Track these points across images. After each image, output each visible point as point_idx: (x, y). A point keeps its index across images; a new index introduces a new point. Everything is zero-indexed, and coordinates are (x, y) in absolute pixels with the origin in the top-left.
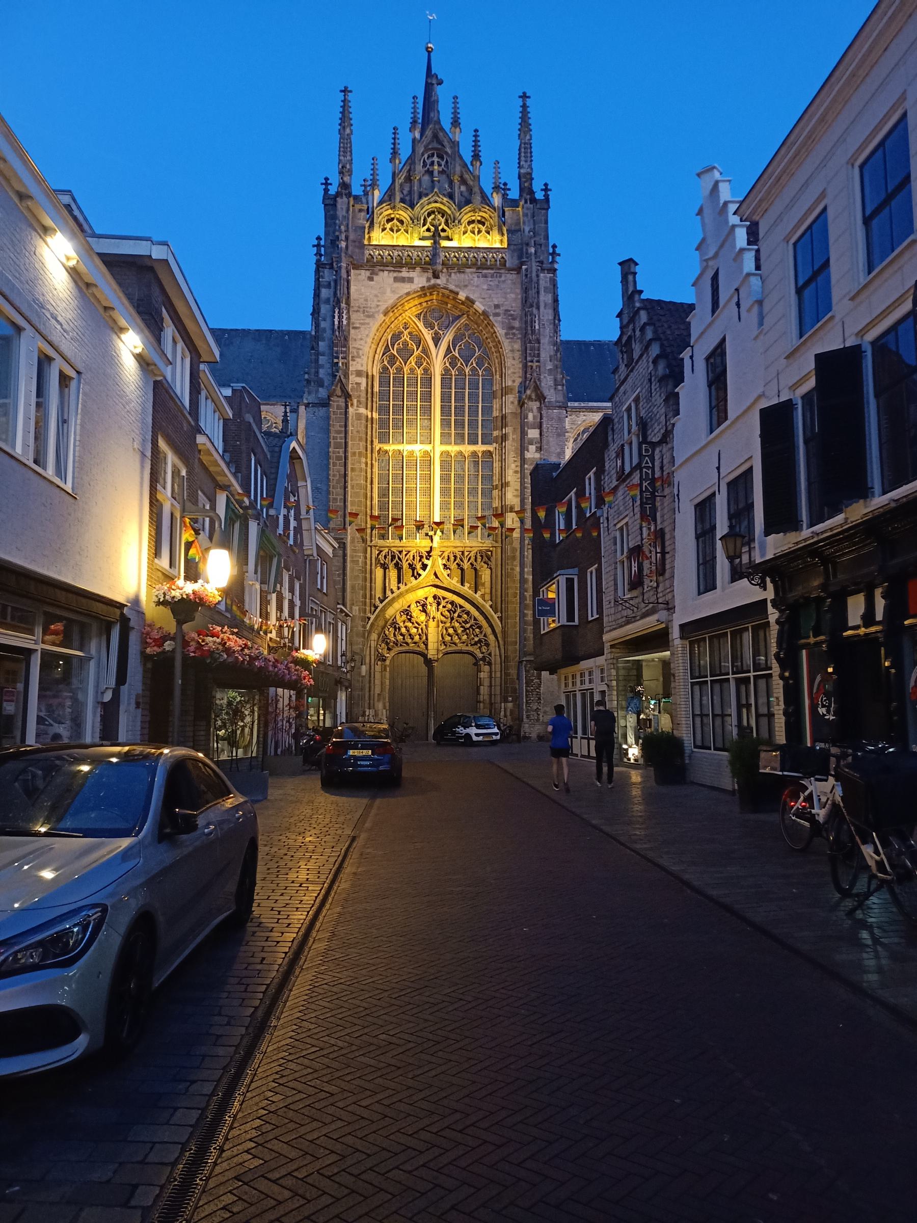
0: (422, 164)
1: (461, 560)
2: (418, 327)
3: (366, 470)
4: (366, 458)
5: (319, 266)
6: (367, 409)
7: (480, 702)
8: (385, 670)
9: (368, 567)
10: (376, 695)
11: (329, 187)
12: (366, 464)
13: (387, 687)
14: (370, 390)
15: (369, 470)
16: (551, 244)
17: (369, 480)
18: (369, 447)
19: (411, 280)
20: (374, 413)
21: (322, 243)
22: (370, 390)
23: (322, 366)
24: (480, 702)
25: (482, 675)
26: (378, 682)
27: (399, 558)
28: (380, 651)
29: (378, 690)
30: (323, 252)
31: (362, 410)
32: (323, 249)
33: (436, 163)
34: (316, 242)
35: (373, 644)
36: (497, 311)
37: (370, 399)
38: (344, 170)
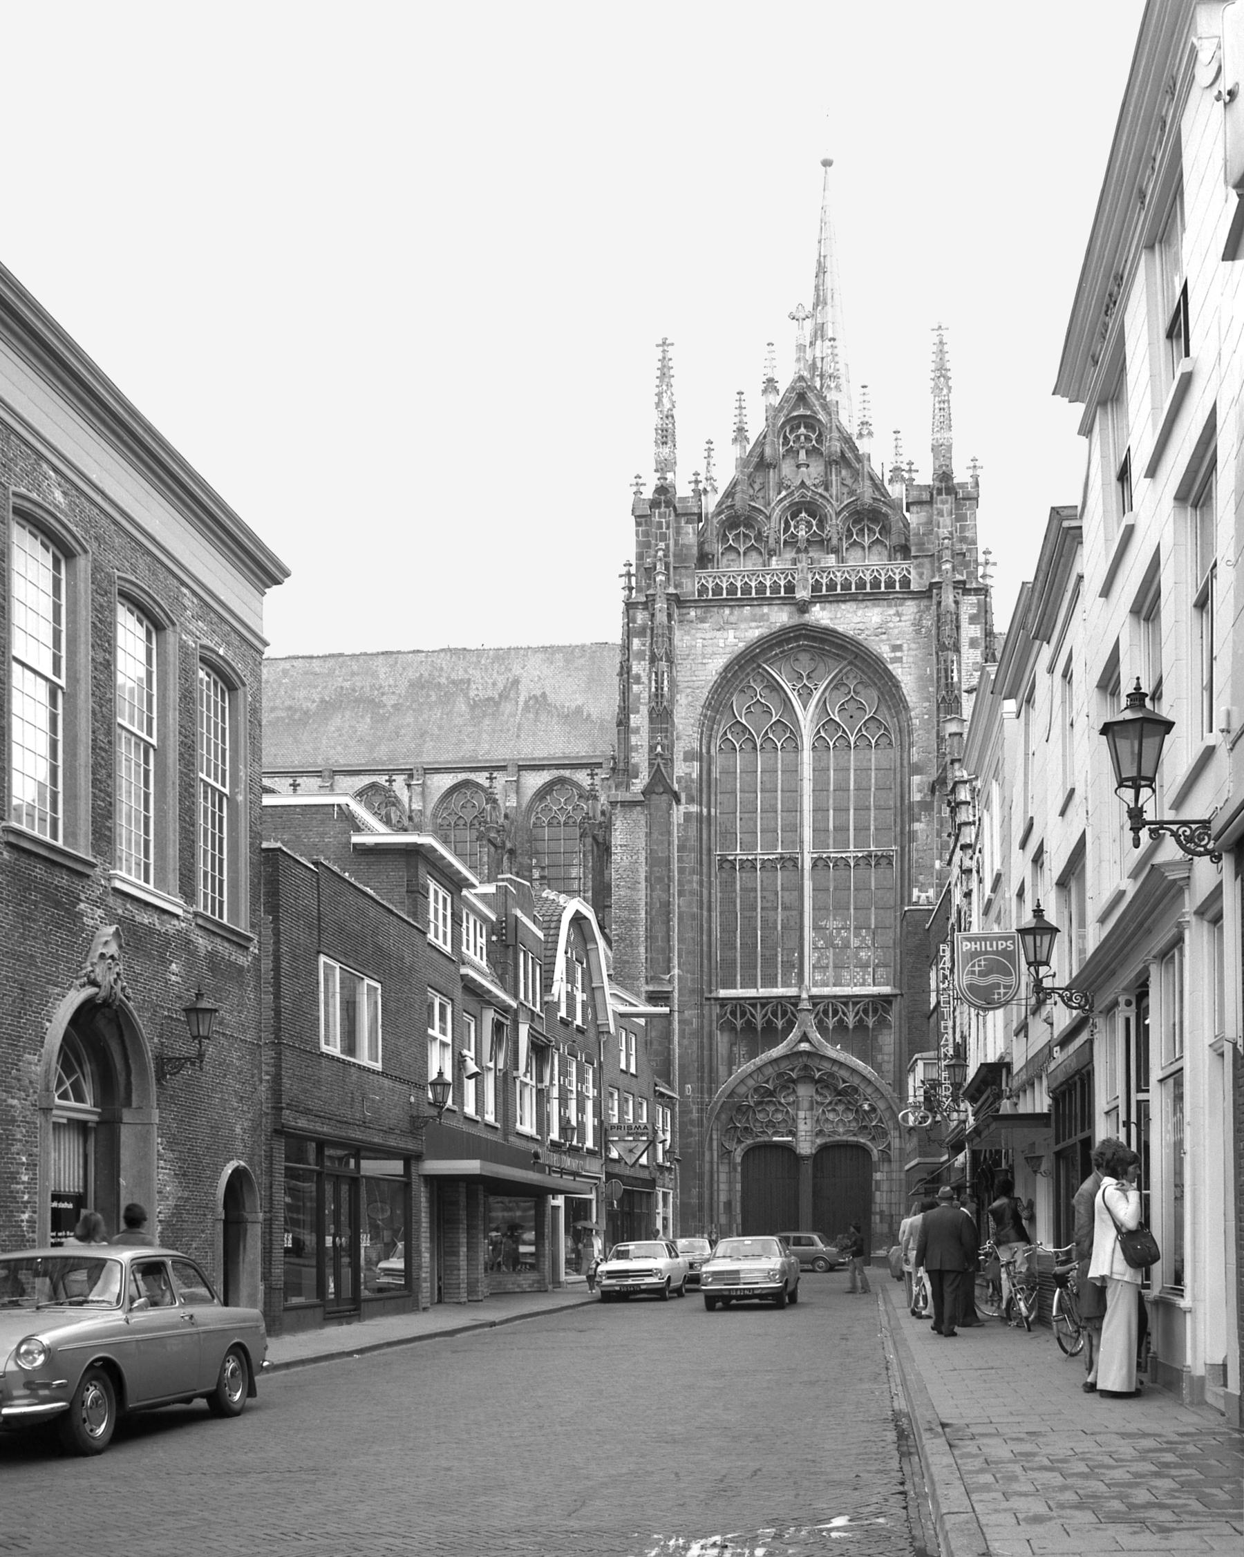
0: (781, 440)
2: (778, 682)
3: (701, 892)
4: (701, 875)
5: (630, 606)
6: (701, 805)
8: (735, 1170)
9: (706, 1029)
10: (721, 1205)
11: (642, 489)
12: (701, 883)
13: (739, 1195)
14: (705, 777)
15: (705, 892)
16: (981, 549)
17: (705, 906)
18: (704, 857)
19: (763, 618)
20: (713, 810)
21: (633, 570)
22: (705, 777)
23: (636, 749)
26: (723, 1187)
29: (723, 1197)
30: (634, 584)
31: (694, 808)
32: (633, 579)
33: (802, 438)
34: (624, 570)
36: (898, 654)
37: (705, 790)
38: (664, 466)
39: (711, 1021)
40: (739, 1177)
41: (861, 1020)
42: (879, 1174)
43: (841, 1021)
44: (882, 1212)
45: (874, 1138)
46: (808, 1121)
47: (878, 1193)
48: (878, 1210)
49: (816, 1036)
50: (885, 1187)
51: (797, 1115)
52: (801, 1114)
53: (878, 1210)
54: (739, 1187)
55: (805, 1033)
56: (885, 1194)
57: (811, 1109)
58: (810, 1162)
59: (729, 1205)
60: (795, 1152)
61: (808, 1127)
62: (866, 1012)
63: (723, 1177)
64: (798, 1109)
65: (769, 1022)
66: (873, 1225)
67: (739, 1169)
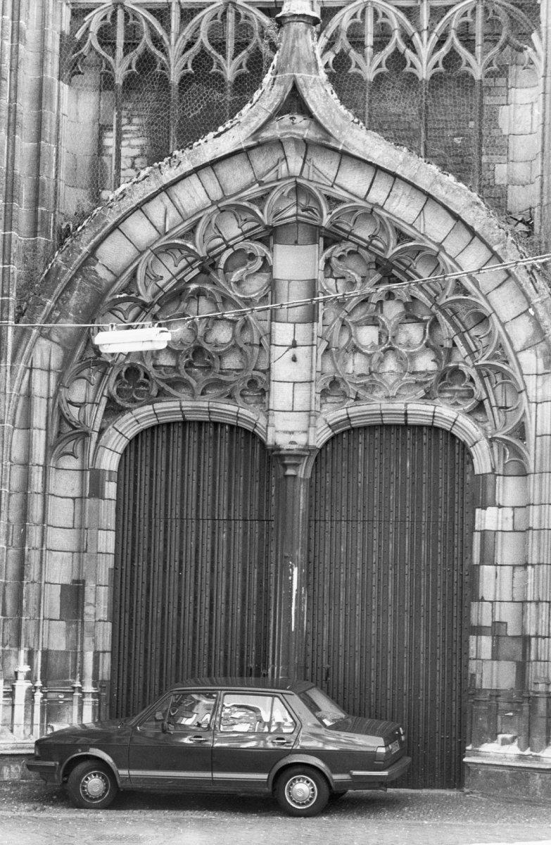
1: (408, 41)
7: (479, 630)
8: (97, 492)
10: (53, 599)
13: (107, 563)
24: (479, 630)
25: (488, 519)
26: (61, 539)
27: (157, 41)
28: (74, 411)
29: (59, 571)
35: (42, 384)
39: (43, 51)
40: (107, 511)
41: (452, 59)
42: (491, 511)
43: (397, 60)
44: (497, 630)
45: (480, 407)
46: (301, 352)
47: (487, 570)
48: (487, 622)
49: (320, 96)
50: (507, 551)
51: (270, 334)
52: (283, 333)
53: (487, 622)
54: (107, 541)
55: (295, 87)
56: (508, 570)
57: (311, 316)
58: (303, 471)
59: (74, 596)
60: (263, 443)
61: (300, 371)
62: (467, 39)
63: (62, 512)
64: (274, 317)
65: (202, 60)
66: (473, 666)
67: (111, 489)
